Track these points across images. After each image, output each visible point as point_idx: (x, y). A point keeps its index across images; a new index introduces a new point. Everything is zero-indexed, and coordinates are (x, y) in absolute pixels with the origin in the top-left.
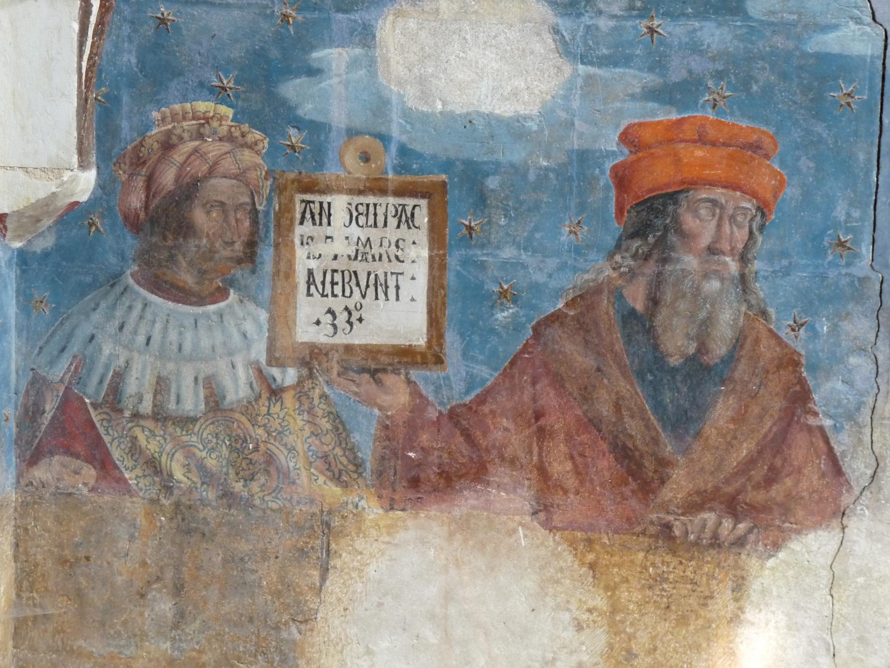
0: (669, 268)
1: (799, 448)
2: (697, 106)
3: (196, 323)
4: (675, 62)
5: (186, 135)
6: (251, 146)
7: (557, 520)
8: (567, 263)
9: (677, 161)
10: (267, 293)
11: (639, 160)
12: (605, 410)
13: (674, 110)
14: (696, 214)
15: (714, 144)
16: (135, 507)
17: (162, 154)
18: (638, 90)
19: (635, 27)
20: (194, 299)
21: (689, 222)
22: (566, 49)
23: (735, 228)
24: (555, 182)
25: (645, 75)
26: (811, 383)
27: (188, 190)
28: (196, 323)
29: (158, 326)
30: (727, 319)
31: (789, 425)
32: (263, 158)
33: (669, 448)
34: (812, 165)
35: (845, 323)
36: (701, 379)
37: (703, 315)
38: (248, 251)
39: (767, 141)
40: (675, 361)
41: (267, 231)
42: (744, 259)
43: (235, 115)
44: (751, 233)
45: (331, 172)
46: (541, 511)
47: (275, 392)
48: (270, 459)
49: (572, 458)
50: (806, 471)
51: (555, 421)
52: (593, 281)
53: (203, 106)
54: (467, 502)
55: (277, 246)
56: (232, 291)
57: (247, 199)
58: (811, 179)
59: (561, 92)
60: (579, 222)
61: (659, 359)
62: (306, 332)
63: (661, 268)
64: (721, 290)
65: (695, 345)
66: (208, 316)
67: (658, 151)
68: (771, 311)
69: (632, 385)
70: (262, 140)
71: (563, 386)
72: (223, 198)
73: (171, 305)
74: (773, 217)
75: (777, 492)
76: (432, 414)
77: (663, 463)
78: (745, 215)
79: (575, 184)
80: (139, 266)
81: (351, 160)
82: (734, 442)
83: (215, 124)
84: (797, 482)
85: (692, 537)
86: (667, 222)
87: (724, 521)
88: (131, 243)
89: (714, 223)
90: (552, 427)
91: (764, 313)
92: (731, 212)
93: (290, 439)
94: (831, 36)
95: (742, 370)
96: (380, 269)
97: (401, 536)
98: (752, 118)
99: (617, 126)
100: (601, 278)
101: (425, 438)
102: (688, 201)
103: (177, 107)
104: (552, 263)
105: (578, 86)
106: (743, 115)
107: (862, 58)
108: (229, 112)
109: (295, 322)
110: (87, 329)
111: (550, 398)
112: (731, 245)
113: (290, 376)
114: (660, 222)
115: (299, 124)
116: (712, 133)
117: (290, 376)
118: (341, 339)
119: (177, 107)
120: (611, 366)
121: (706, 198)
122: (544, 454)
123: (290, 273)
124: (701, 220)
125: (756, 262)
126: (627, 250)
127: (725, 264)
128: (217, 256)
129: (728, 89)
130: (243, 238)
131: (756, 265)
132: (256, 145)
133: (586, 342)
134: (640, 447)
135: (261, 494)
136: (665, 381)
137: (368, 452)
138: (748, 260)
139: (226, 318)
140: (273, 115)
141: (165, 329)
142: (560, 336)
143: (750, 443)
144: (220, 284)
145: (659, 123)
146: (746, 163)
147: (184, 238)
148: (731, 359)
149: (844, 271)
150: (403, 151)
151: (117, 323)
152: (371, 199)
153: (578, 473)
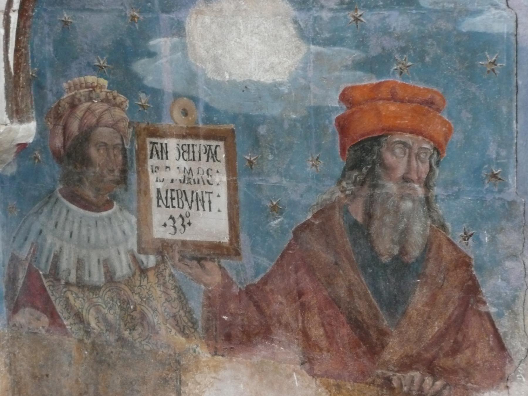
0: (377, 191)
1: (474, 328)
2: (389, 73)
3: (96, 224)
4: (373, 42)
5: (83, 99)
6: (120, 105)
7: (317, 369)
8: (311, 187)
9: (378, 113)
10: (134, 205)
11: (353, 113)
12: (343, 293)
13: (374, 76)
14: (393, 154)
15: (402, 101)
16: (70, 343)
17: (71, 111)
18: (350, 63)
19: (345, 17)
20: (94, 208)
21: (389, 158)
22: (302, 34)
23: (420, 164)
24: (301, 130)
25: (354, 51)
26: (479, 280)
27: (86, 136)
28: (96, 224)
29: (76, 225)
30: (419, 231)
31: (466, 310)
32: (126, 114)
33: (386, 323)
34: (470, 116)
35: (501, 235)
36: (404, 274)
37: (402, 226)
38: (123, 176)
39: (438, 98)
40: (385, 259)
41: (132, 163)
42: (427, 186)
43: (109, 84)
44: (431, 166)
45: (166, 123)
46: (306, 362)
47: (144, 271)
48: (143, 316)
49: (323, 325)
50: (479, 345)
51: (311, 299)
52: (329, 199)
53: (91, 79)
54: (261, 353)
55: (138, 172)
56: (115, 203)
57: (119, 141)
58: (470, 127)
59: (301, 65)
60: (318, 158)
61: (375, 257)
62: (160, 232)
63: (372, 192)
64: (414, 209)
65: (398, 248)
66: (102, 219)
67: (365, 107)
68: (448, 224)
69: (358, 275)
70: (125, 101)
71: (314, 274)
72: (106, 141)
73: (82, 211)
74: (445, 155)
75: (461, 359)
76: (235, 290)
77: (383, 333)
78: (426, 153)
79: (314, 130)
80: (63, 185)
81: (177, 114)
82: (429, 321)
83: (98, 91)
84: (474, 354)
85: (405, 389)
86: (375, 158)
87: (426, 378)
88: (57, 170)
89: (406, 159)
90: (309, 303)
91: (443, 227)
92: (416, 151)
93: (154, 303)
94: (478, 19)
95: (431, 268)
96: (199, 189)
97: (223, 374)
98: (426, 82)
99: (338, 89)
100: (334, 197)
101: (232, 306)
102: (387, 143)
103: (76, 80)
104: (303, 186)
105: (312, 60)
106: (421, 80)
107: (500, 36)
108: (104, 82)
109: (152, 224)
110: (36, 227)
111: (307, 283)
112: (418, 175)
113: (151, 261)
114: (369, 158)
115: (146, 89)
116: (400, 93)
117: (151, 261)
118: (179, 237)
119: (76, 80)
120: (344, 261)
121: (398, 141)
122: (306, 322)
123: (147, 192)
124: (396, 157)
125: (435, 188)
126: (349, 178)
127: (414, 189)
128: (105, 179)
129: (409, 61)
130: (119, 167)
131: (436, 191)
132: (122, 105)
133: (328, 243)
134: (366, 321)
135: (139, 340)
136: (380, 274)
137: (199, 314)
138: (430, 186)
139: (113, 220)
140: (128, 83)
141: (80, 227)
142: (310, 239)
143: (440, 322)
144: (108, 198)
145: (365, 86)
146: (424, 115)
147: (87, 166)
148: (423, 259)
149: (497, 196)
150: (208, 108)
151: (53, 223)
152: (190, 142)
153: (328, 337)
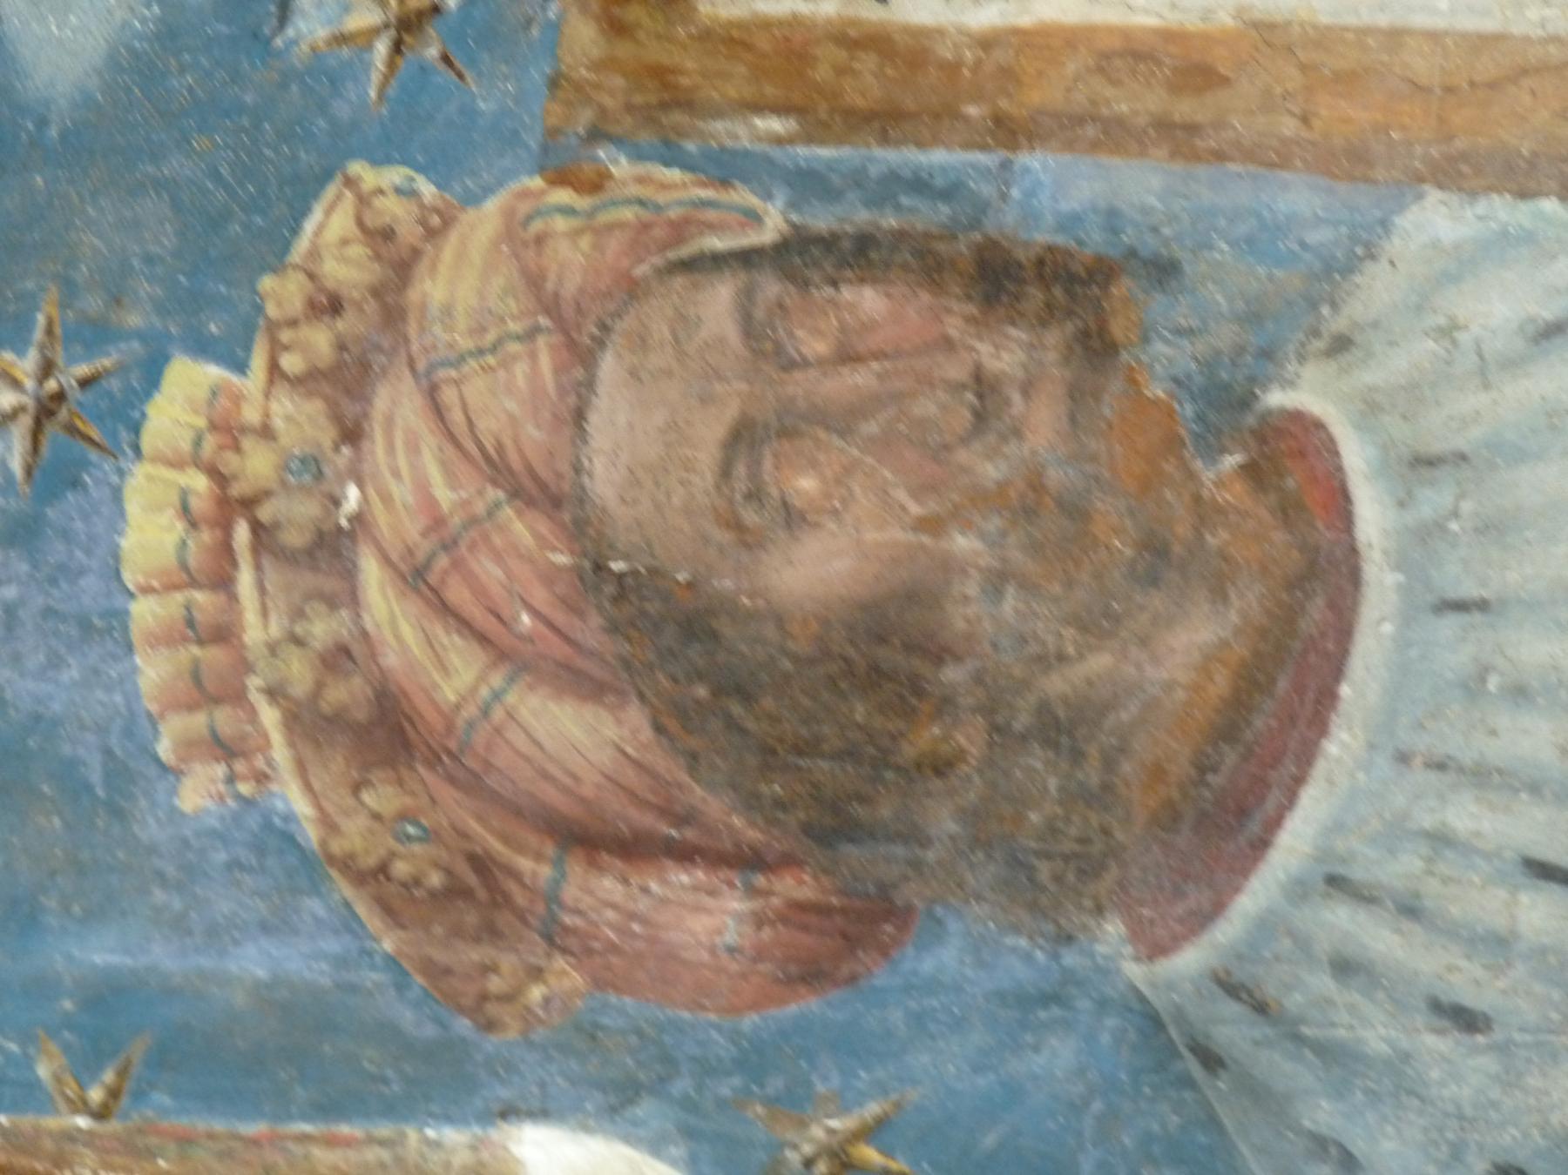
3: (1460, 606)
5: (323, 629)
6: (397, 260)
10: (1298, 198)
17: (433, 761)
20: (1317, 609)
27: (654, 625)
28: (1460, 606)
29: (1465, 815)
32: (473, 199)
38: (1035, 296)
41: (919, 184)
43: (203, 348)
53: (150, 524)
55: (1009, 132)
56: (1276, 398)
57: (717, 302)
66: (1424, 538)
70: (363, 201)
72: (711, 430)
73: (1341, 745)
80: (1099, 910)
83: (257, 465)
88: (962, 953)
103: (153, 672)
109: (1482, 43)
119: (153, 672)
128: (1055, 476)
130: (954, 327)
132: (387, 234)
139: (1437, 430)
141: (1483, 777)
144: (1231, 461)
147: (940, 654)
151: (1437, 1044)
